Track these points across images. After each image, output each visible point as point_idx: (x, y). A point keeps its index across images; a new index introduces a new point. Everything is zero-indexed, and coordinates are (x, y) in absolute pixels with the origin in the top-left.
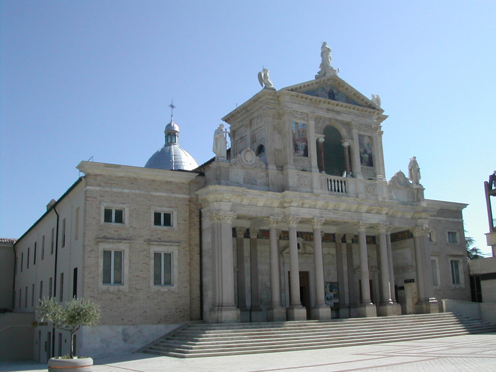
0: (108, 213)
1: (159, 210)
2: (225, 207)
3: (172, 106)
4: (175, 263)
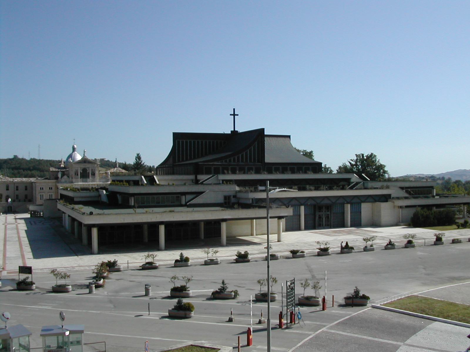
0: (41, 188)
1: (50, 187)
3: (74, 139)
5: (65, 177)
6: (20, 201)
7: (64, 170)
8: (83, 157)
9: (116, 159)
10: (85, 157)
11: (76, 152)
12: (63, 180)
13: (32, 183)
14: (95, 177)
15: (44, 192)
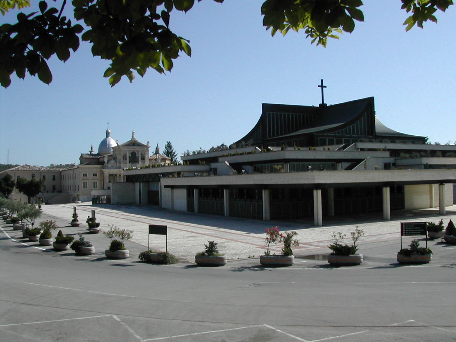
0: (84, 175)
2: (107, 173)
3: (108, 123)
4: (98, 183)
5: (112, 162)
6: (47, 192)
7: (99, 157)
8: (132, 139)
9: (157, 144)
10: (135, 139)
11: (110, 138)
12: (110, 165)
13: (60, 172)
14: (145, 162)
15: (88, 179)
